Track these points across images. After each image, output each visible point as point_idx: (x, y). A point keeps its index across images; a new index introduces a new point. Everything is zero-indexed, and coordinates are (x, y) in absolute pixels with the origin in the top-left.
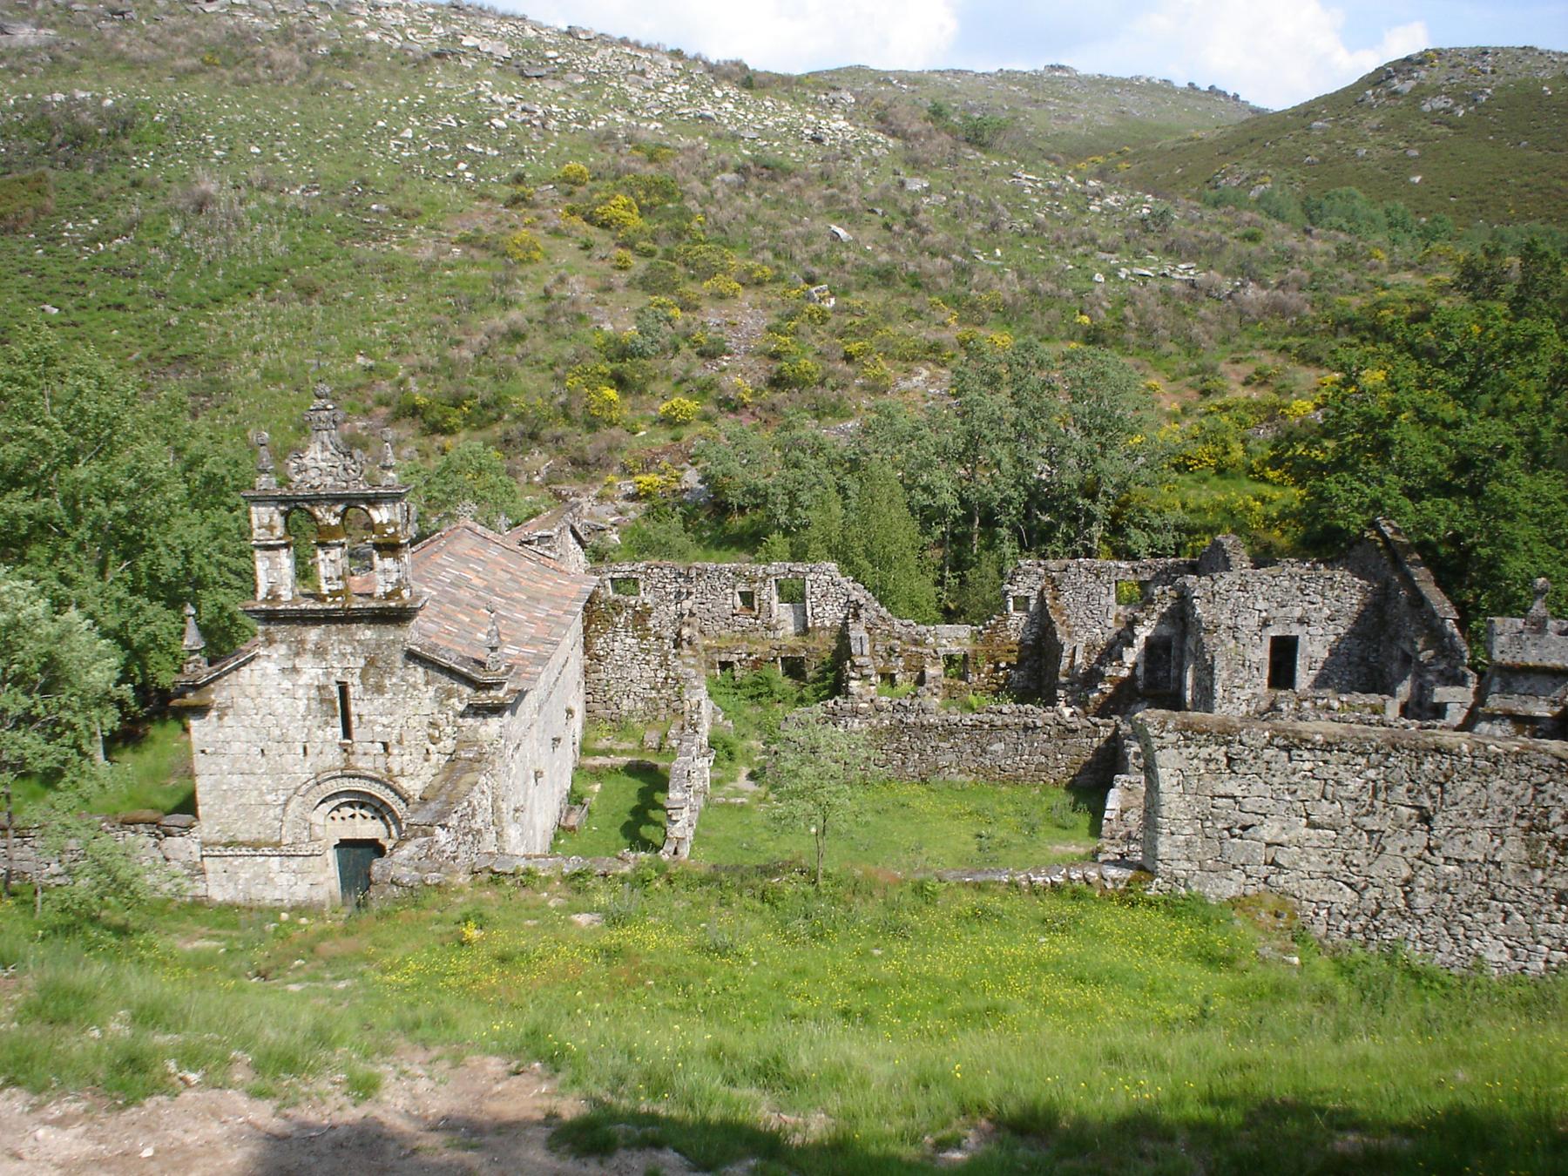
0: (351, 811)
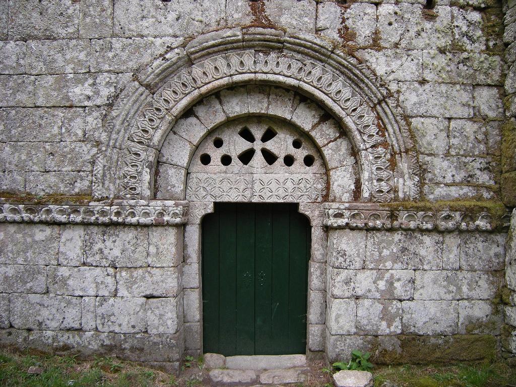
0: (243, 145)
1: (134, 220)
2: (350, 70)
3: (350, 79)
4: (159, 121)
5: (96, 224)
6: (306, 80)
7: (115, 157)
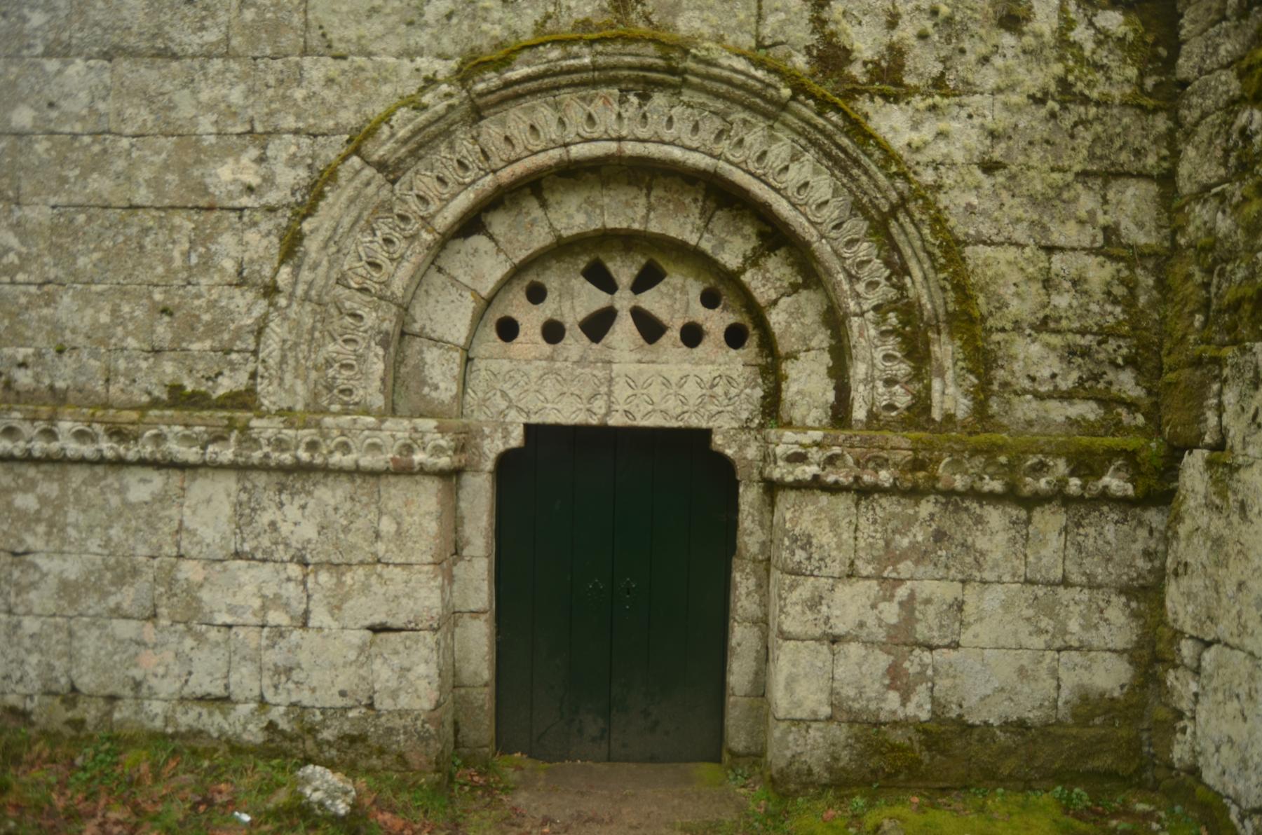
0: (591, 299)
1: (347, 460)
2: (829, 137)
3: (828, 155)
4: (404, 244)
5: (264, 467)
6: (731, 158)
7: (308, 321)
